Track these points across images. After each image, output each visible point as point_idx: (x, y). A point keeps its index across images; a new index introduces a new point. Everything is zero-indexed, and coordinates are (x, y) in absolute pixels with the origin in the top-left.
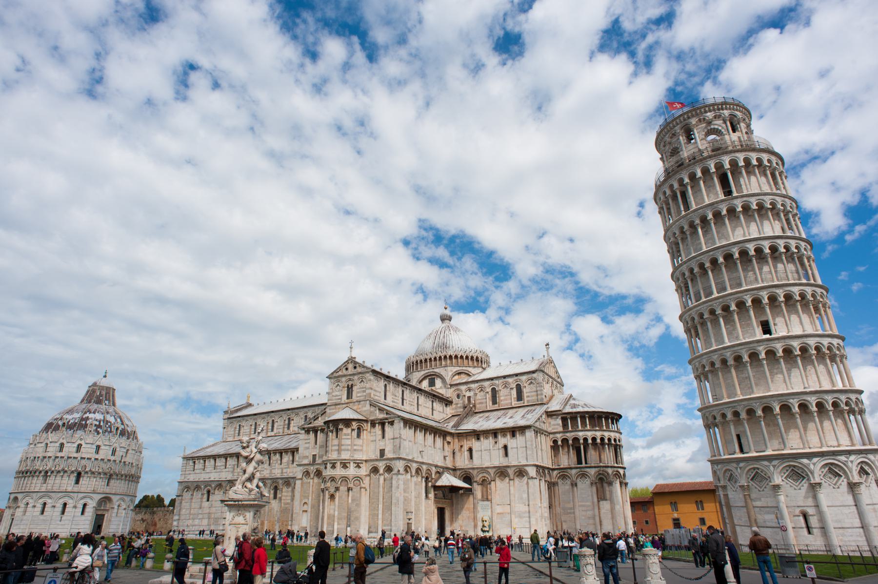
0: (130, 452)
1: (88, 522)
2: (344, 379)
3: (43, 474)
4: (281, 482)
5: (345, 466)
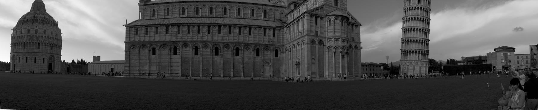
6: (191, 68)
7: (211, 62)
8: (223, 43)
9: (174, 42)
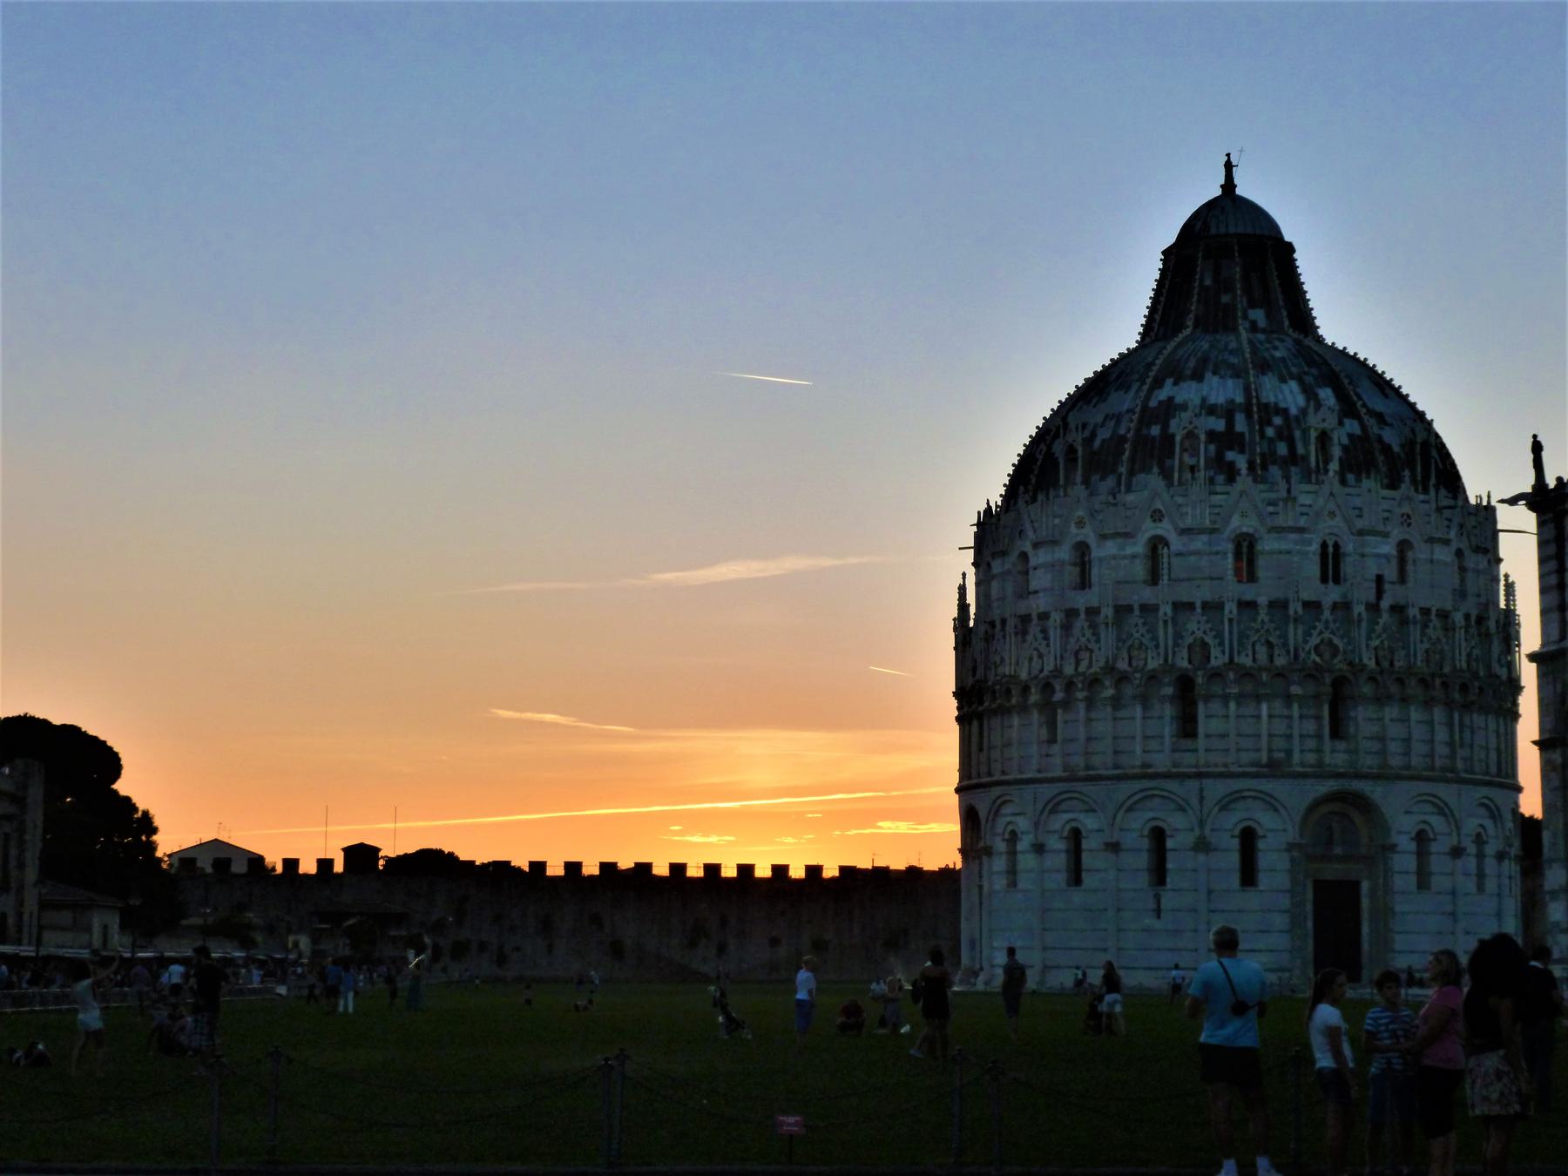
0: (1420, 552)
1: (1280, 921)
3: (1034, 697)
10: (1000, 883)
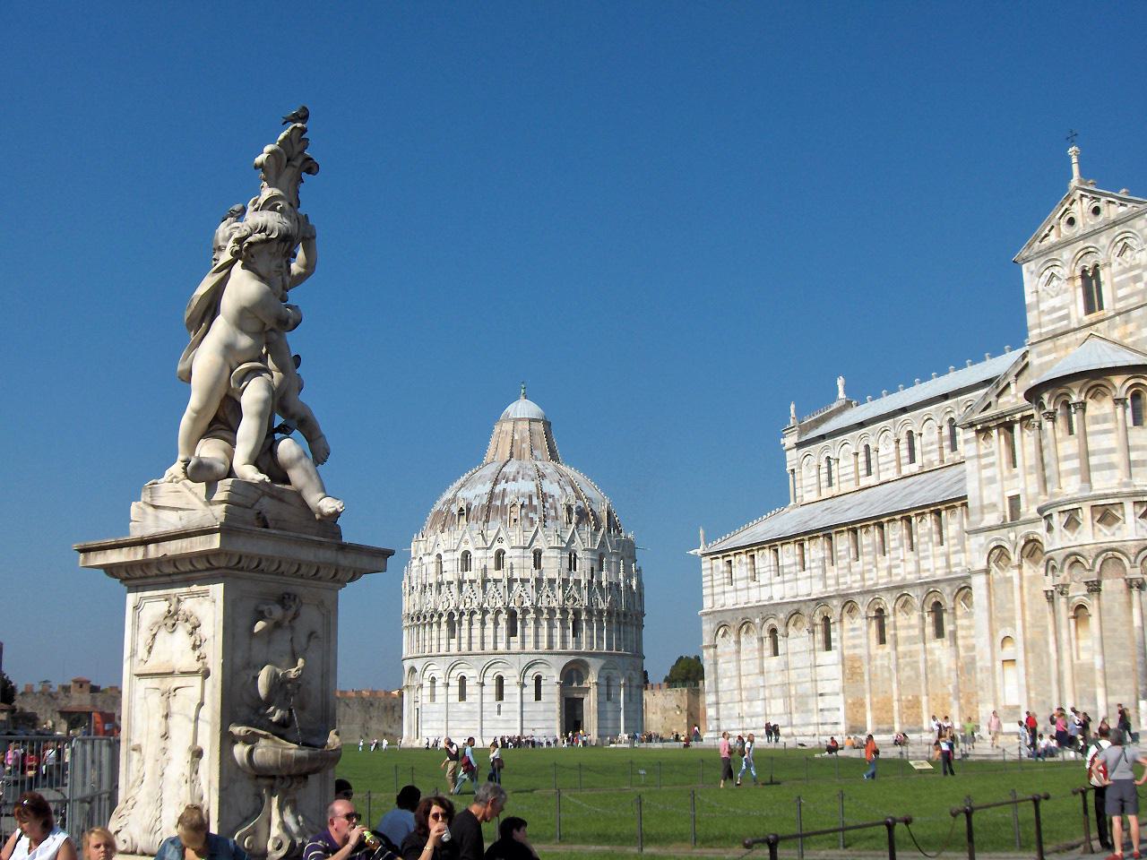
2: (1067, 254)
3: (444, 619)
4: (948, 590)
5: (1106, 515)
6: (868, 696)
7: (922, 666)
8: (949, 581)
9: (818, 601)
10: (426, 700)
